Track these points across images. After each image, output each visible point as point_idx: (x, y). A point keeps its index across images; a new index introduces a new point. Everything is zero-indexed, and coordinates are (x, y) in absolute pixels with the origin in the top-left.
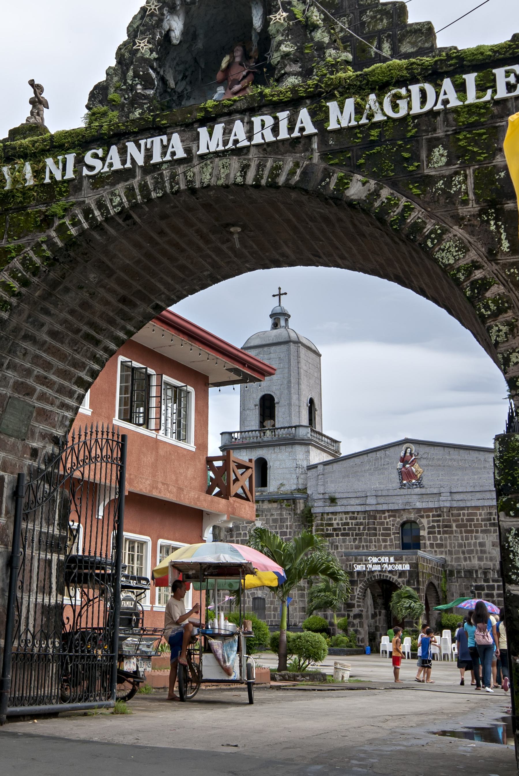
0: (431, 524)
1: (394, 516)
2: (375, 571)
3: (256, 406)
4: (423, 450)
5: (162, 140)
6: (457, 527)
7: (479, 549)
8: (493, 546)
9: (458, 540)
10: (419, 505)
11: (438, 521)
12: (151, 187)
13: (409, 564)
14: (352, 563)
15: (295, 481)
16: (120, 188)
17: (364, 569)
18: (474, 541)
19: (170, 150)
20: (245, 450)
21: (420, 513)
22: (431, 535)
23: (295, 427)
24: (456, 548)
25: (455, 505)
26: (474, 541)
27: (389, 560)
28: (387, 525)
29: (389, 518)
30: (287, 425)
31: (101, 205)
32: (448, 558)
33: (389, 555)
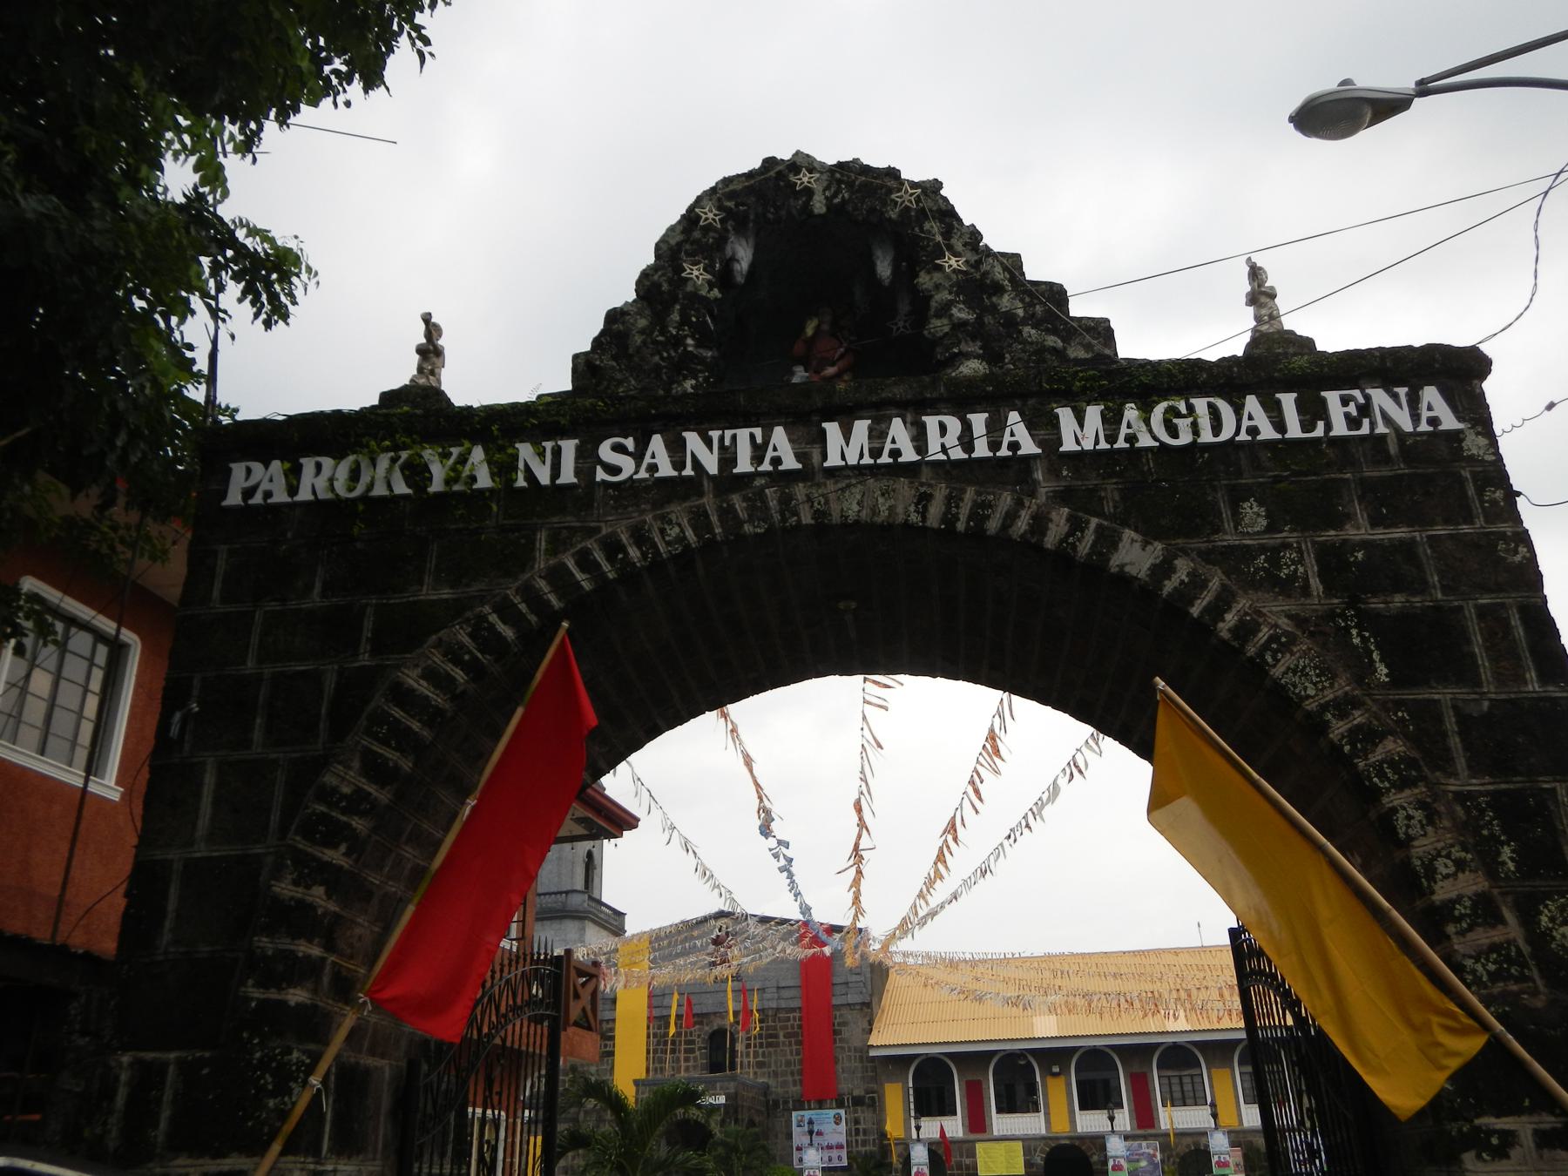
1: (701, 1023)
5: (752, 436)
6: (785, 1037)
9: (785, 1055)
12: (743, 515)
16: (679, 512)
19: (770, 454)
23: (567, 893)
25: (783, 1006)
30: (555, 890)
31: (640, 537)
32: (772, 1082)
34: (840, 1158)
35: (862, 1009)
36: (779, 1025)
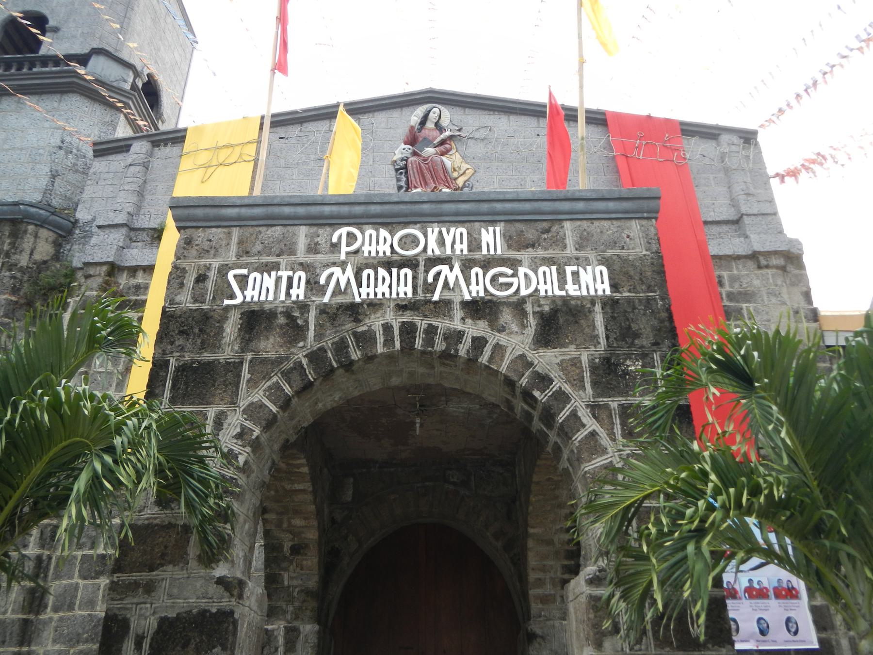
2: (374, 305)
13: (605, 261)
15: (44, 182)
17: (299, 292)
27: (474, 244)
34: (792, 627)
35: (783, 269)
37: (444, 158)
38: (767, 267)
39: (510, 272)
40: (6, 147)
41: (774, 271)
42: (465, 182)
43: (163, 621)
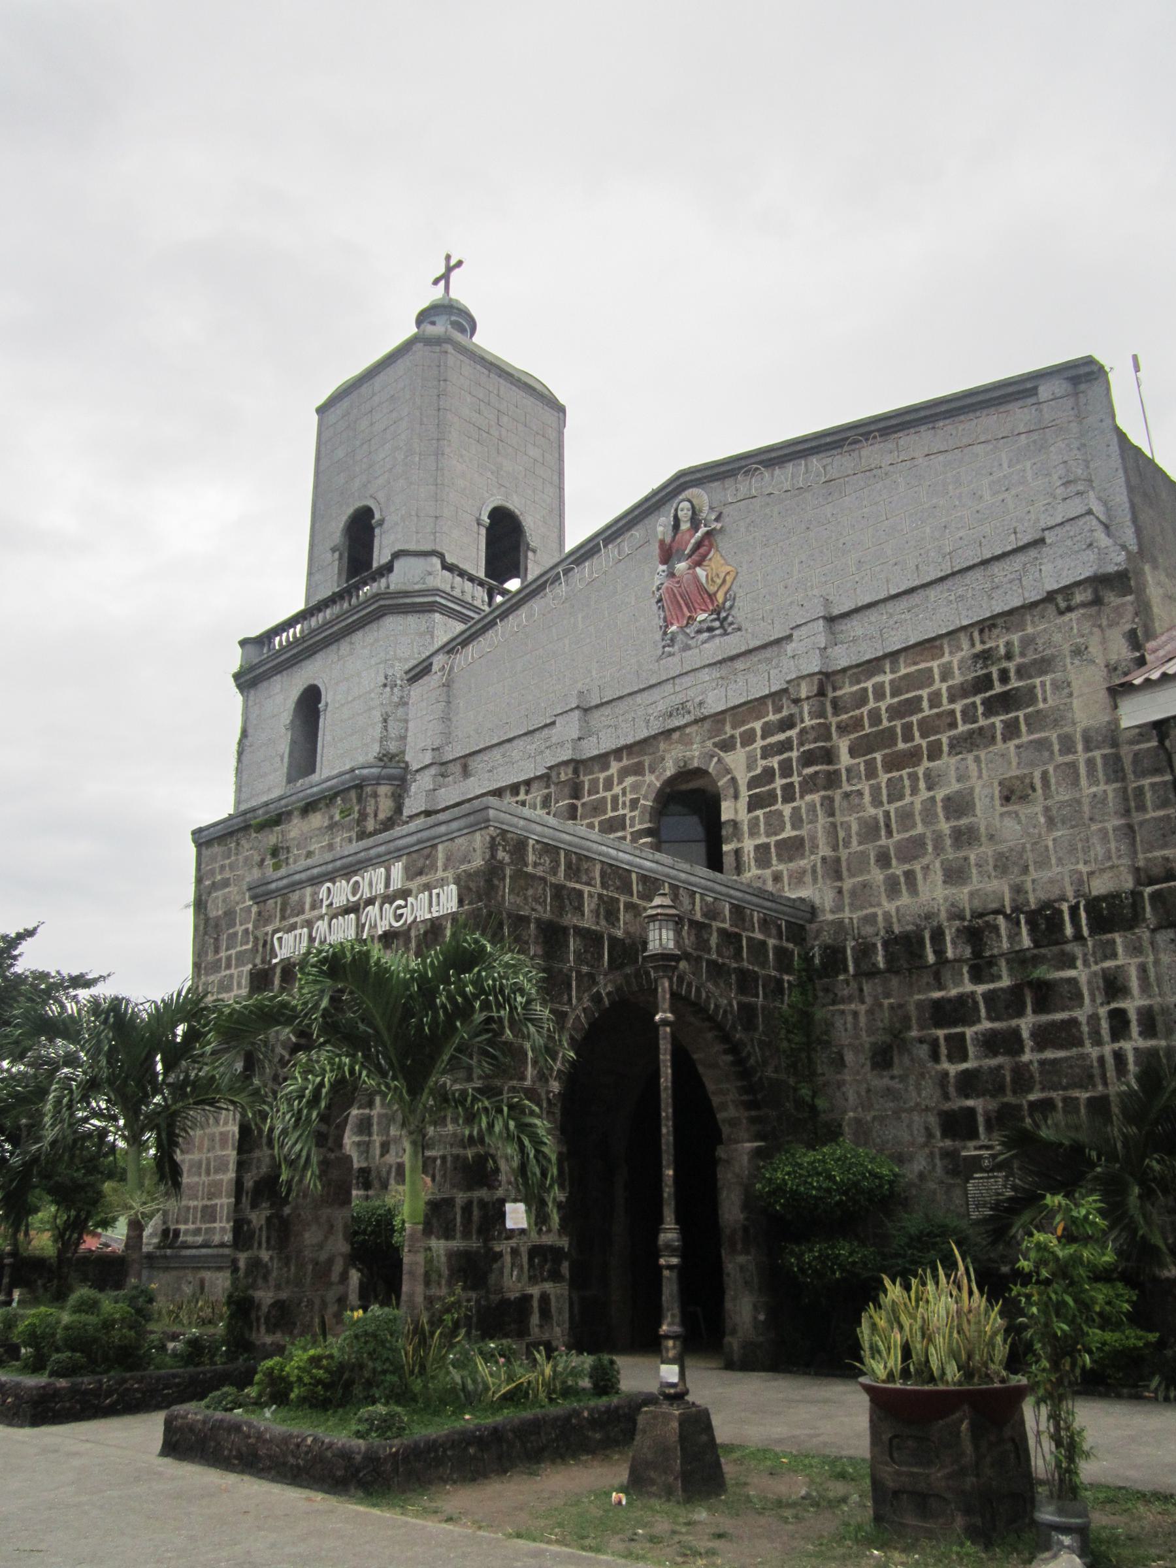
0: (761, 763)
1: (637, 770)
3: (333, 550)
4: (727, 492)
6: (853, 752)
7: (945, 826)
8: (1007, 799)
9: (860, 807)
10: (716, 703)
11: (786, 746)
14: (269, 929)
15: (378, 731)
18: (924, 794)
20: (279, 676)
21: (720, 731)
22: (759, 813)
24: (855, 846)
25: (843, 663)
26: (924, 794)
28: (615, 809)
29: (620, 782)
33: (384, 861)
35: (1097, 601)
36: (834, 720)
37: (698, 570)
38: (1070, 609)
39: (401, 902)
40: (350, 699)
41: (1082, 611)
42: (726, 594)
43: (255, 1182)
